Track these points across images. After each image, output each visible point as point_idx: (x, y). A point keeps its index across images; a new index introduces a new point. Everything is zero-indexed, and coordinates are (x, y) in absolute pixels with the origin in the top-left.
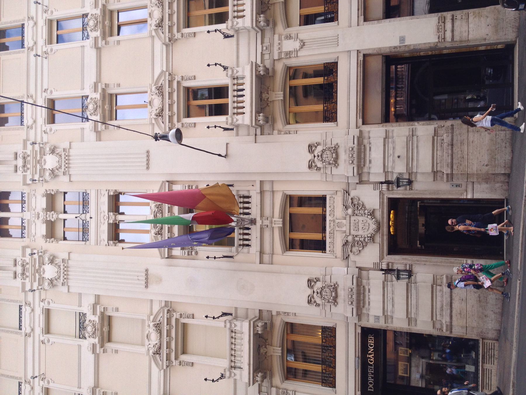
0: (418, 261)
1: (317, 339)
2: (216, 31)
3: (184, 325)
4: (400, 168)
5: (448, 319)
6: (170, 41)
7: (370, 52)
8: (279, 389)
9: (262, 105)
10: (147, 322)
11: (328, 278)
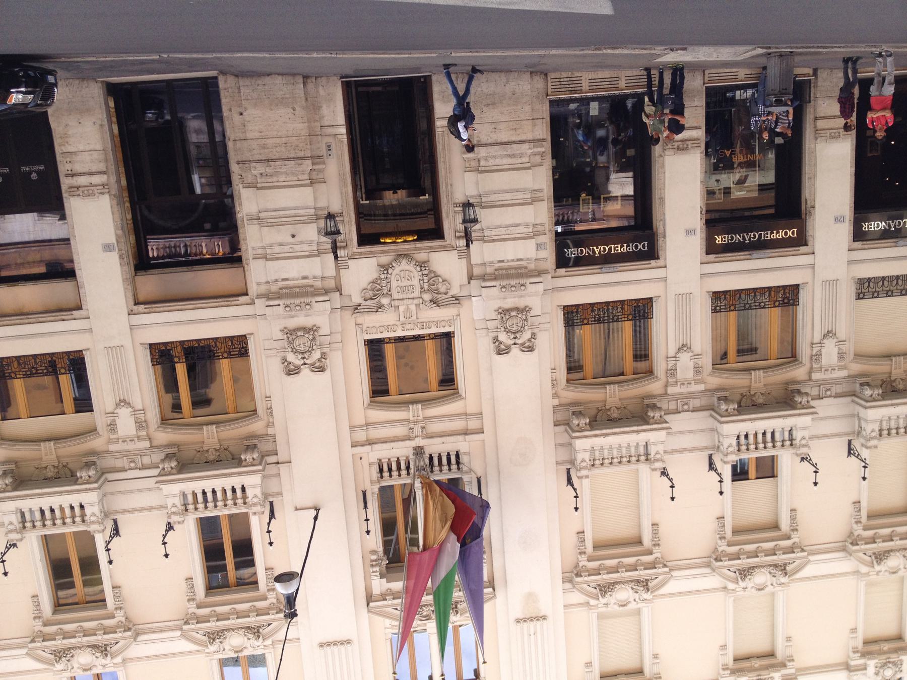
0: (447, 196)
1: (586, 333)
2: (108, 550)
3: (595, 547)
4: (311, 233)
5: (525, 146)
6: (129, 629)
7: (130, 295)
8: (667, 382)
9: (227, 458)
10: (601, 610)
11: (491, 325)
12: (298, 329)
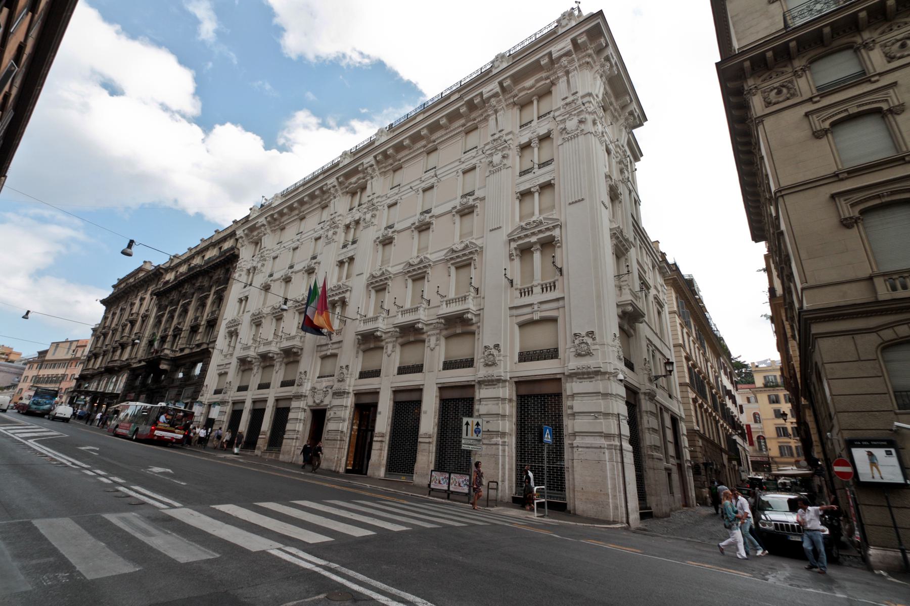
12: (584, 355)
